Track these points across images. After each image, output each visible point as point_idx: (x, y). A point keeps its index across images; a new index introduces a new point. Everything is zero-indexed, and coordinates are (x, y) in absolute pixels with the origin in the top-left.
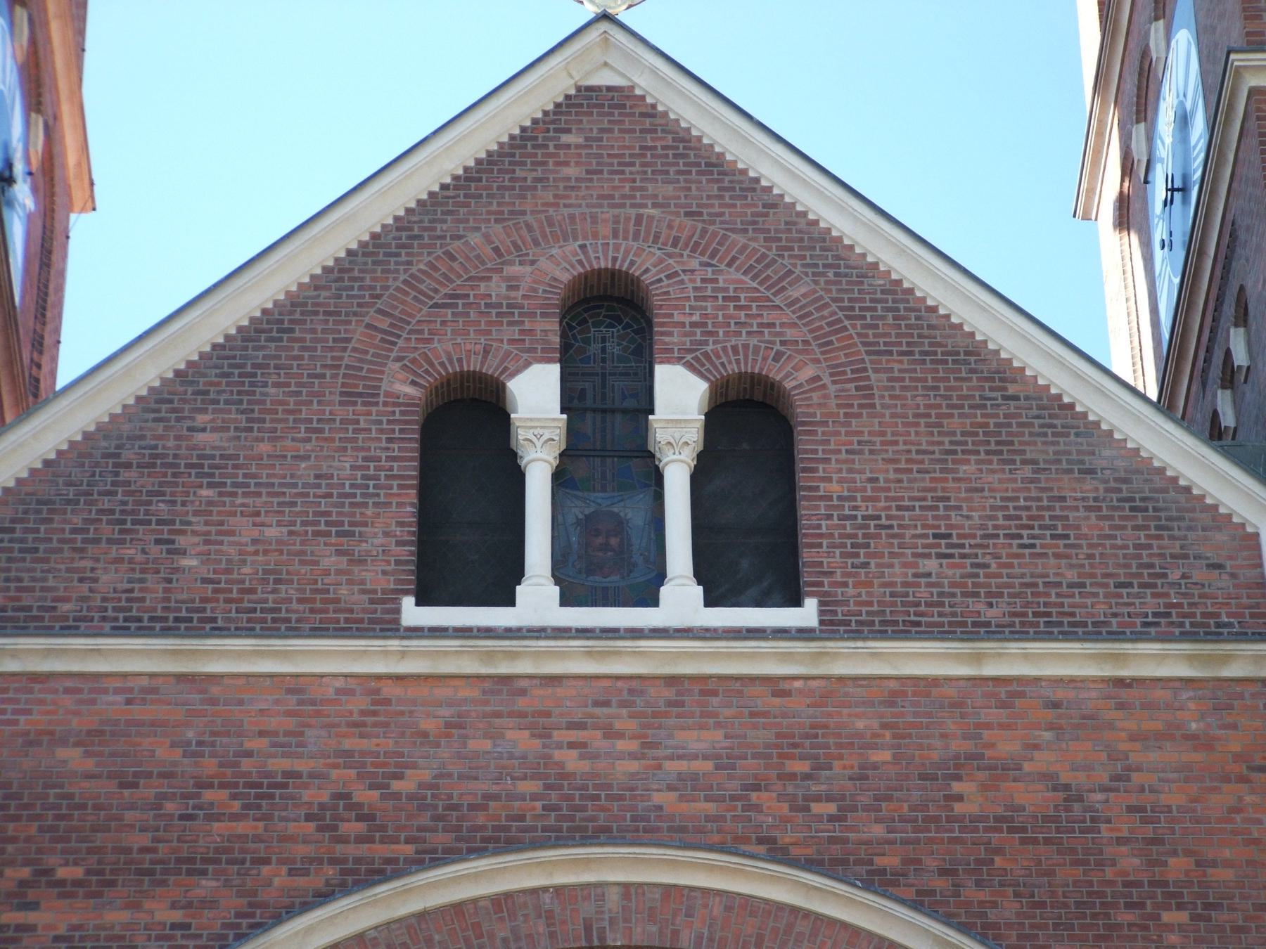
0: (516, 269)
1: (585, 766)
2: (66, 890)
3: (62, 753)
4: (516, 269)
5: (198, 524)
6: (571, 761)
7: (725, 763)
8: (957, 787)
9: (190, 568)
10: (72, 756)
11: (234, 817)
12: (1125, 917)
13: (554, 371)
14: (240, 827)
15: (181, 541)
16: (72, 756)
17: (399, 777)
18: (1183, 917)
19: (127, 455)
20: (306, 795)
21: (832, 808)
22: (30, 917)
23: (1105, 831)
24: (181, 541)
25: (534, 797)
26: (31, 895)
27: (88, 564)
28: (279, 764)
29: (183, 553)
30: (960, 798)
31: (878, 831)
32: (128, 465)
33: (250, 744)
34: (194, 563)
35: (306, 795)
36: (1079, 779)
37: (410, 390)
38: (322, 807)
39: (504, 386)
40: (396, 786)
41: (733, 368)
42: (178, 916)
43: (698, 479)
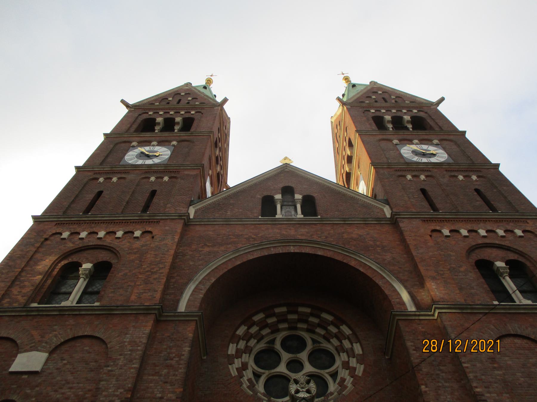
0: (275, 186)
1: (287, 233)
2: (208, 246)
3: (209, 232)
4: (275, 186)
5: (230, 210)
6: (285, 233)
7: (308, 233)
8: (343, 235)
9: (229, 214)
10: (211, 233)
11: (234, 239)
12: (370, 248)
13: (281, 195)
14: (235, 240)
15: (228, 211)
16: (211, 233)
17: (259, 234)
18: (380, 248)
19: (221, 203)
20: (245, 236)
21: (325, 237)
22: (204, 249)
23: (367, 240)
24: (228, 211)
25: (279, 236)
26: (204, 247)
27: (214, 214)
28: (241, 233)
29: (228, 212)
30: (344, 236)
31: (332, 239)
32: (221, 204)
33: (236, 231)
34: (229, 213)
35: (245, 236)
36: (362, 234)
37: (260, 197)
38: (247, 238)
39: (273, 196)
40: (258, 235)
41: (306, 194)
42: (225, 249)
43: (301, 207)
